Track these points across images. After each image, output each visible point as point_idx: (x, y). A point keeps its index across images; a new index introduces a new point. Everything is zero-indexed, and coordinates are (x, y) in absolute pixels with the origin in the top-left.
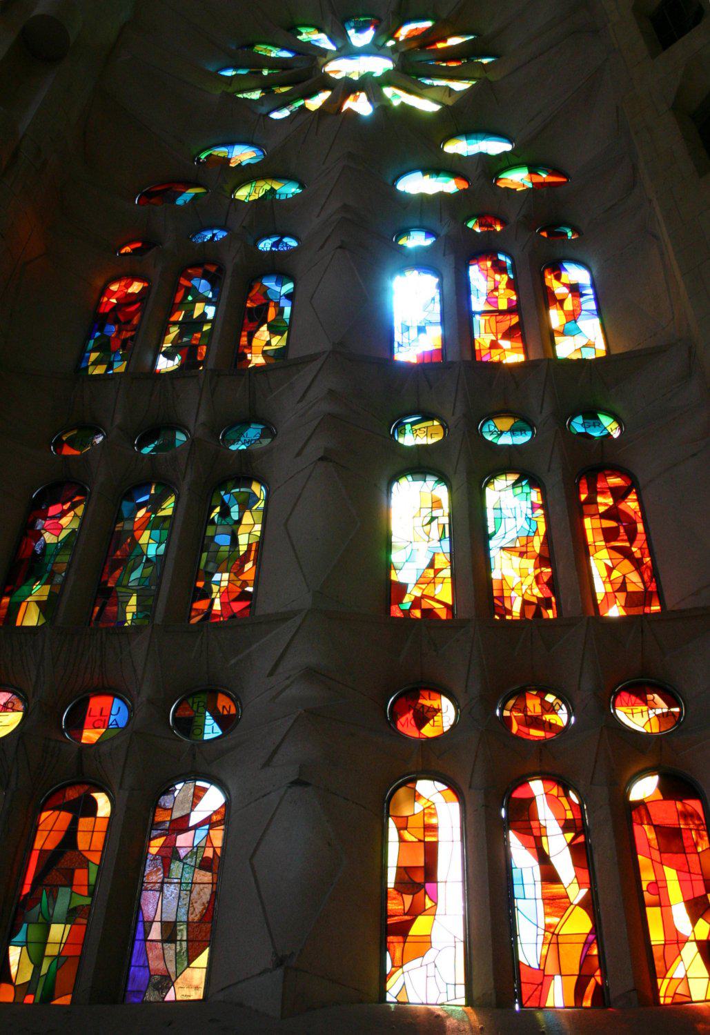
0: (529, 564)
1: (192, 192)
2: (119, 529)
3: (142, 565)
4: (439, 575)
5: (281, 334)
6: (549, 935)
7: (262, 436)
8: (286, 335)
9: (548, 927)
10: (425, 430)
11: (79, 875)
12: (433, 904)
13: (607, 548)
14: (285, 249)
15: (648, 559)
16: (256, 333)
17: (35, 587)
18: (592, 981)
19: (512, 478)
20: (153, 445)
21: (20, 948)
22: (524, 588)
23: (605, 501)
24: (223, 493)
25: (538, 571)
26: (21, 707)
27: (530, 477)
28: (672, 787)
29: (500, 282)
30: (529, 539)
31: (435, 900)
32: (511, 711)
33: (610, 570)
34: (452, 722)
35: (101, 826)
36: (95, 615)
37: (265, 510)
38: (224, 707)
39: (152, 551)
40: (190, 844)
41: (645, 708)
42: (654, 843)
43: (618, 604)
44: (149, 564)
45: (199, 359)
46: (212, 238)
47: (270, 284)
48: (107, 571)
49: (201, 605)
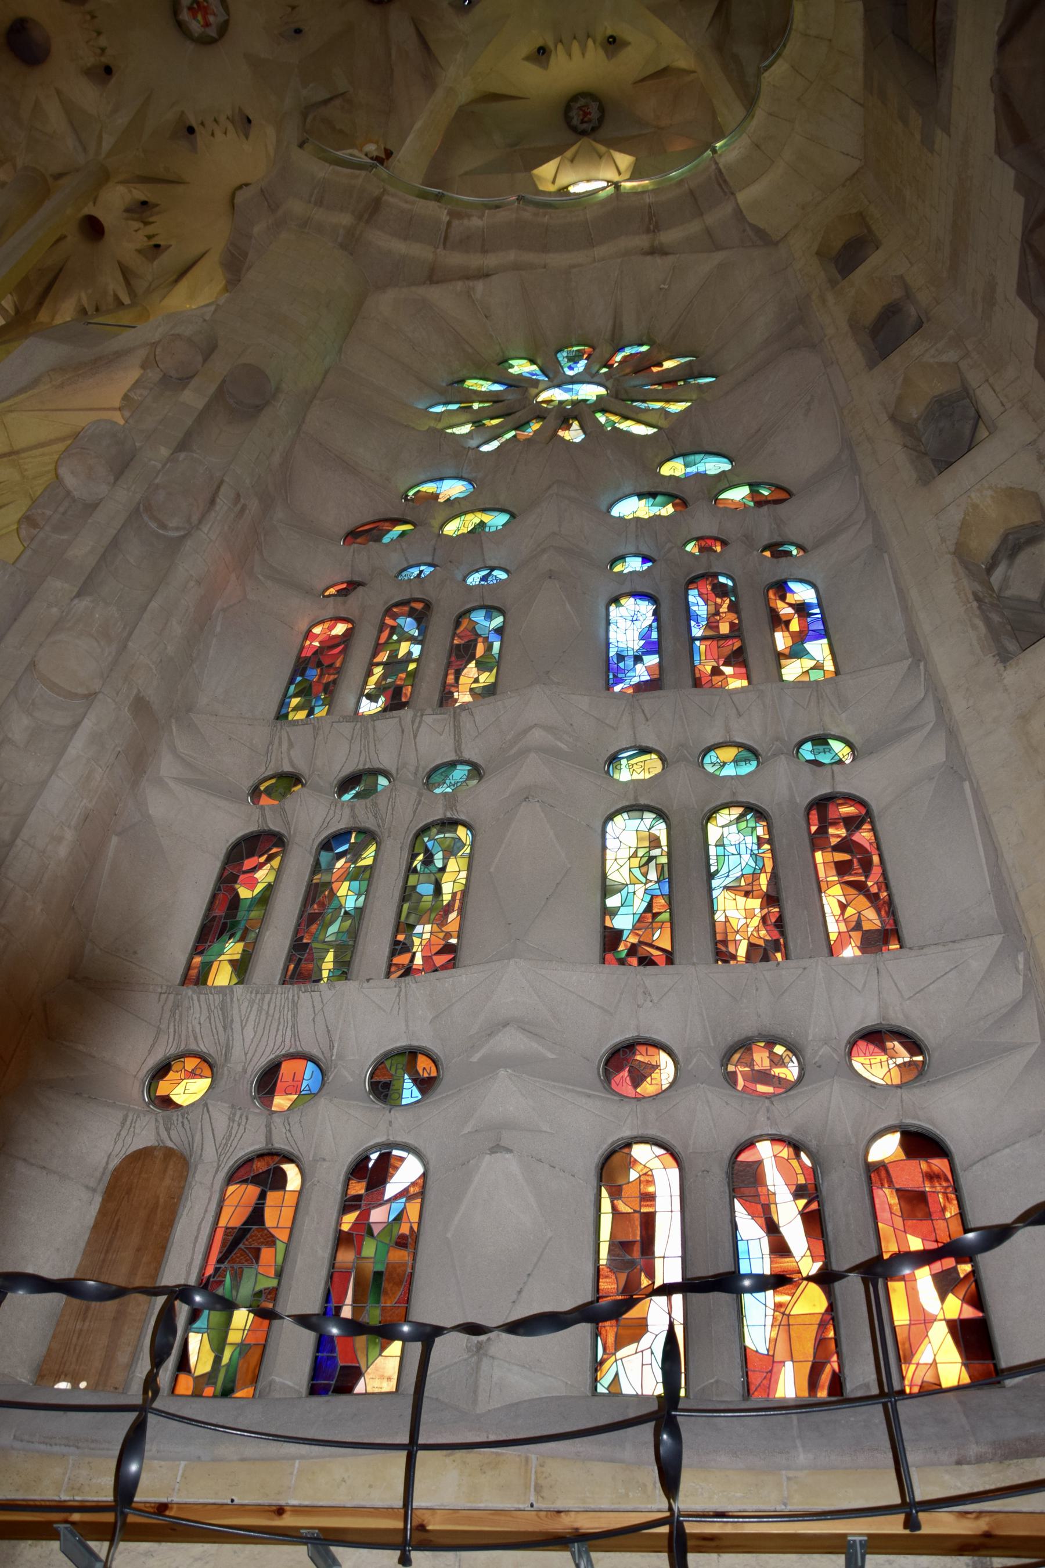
0: (755, 904)
1: (400, 529)
2: (318, 881)
3: (340, 918)
5: (491, 671)
7: (469, 778)
8: (495, 671)
11: (266, 1253)
14: (495, 582)
15: (885, 894)
16: (463, 669)
20: (354, 792)
21: (200, 1335)
22: (750, 930)
23: (836, 833)
24: (426, 839)
25: (765, 911)
29: (721, 606)
30: (755, 876)
32: (736, 1066)
33: (843, 907)
34: (671, 1079)
35: (290, 1200)
36: (289, 973)
37: (471, 857)
38: (424, 1068)
39: (350, 904)
41: (884, 1058)
42: (896, 1209)
43: (853, 944)
45: (403, 700)
46: (419, 575)
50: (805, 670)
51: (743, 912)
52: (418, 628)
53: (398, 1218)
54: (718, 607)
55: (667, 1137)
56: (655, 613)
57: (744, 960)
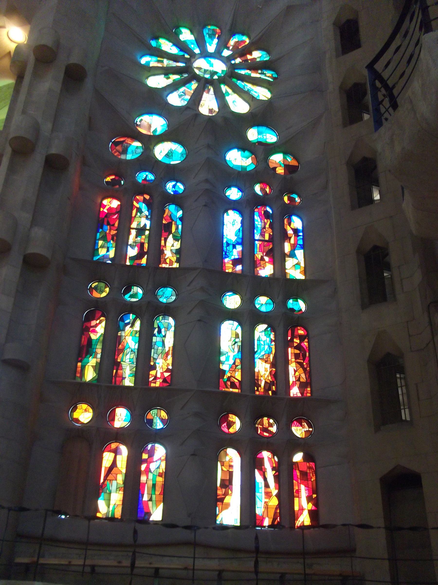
0: (268, 366)
2: (120, 335)
4: (237, 368)
5: (178, 240)
6: (265, 505)
9: (265, 502)
12: (231, 492)
13: (295, 362)
17: (90, 359)
19: (265, 326)
22: (266, 376)
25: (271, 369)
26: (91, 410)
27: (272, 327)
28: (308, 458)
31: (232, 491)
32: (258, 425)
33: (295, 371)
38: (163, 416)
41: (301, 428)
44: (132, 353)
47: (172, 208)
48: (117, 354)
49: (153, 373)
50: (294, 264)
52: (148, 211)
53: (158, 468)
54: (265, 224)
56: (242, 222)
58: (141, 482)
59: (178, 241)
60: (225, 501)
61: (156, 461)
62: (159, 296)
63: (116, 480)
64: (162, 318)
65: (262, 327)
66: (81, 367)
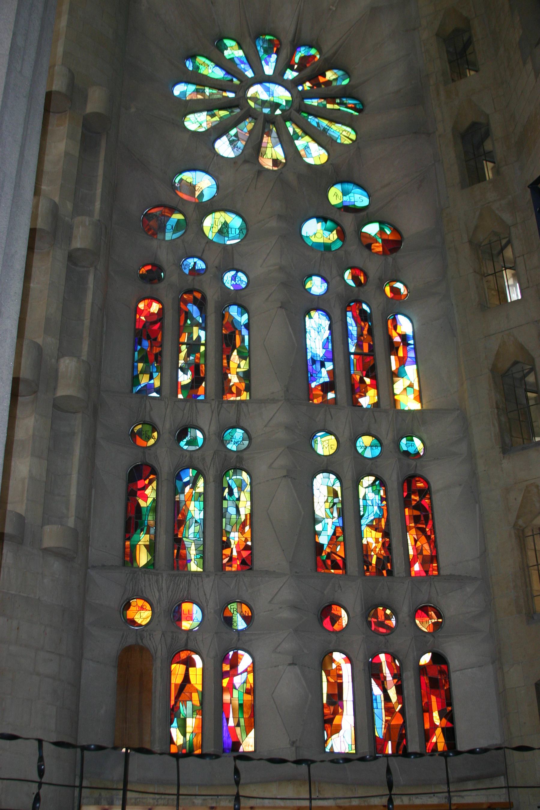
0: (379, 535)
2: (178, 499)
3: (194, 524)
10: (328, 442)
18: (402, 744)
19: (372, 479)
22: (377, 549)
25: (384, 540)
26: (148, 607)
30: (379, 520)
31: (342, 708)
33: (416, 541)
34: (346, 623)
35: (200, 672)
36: (175, 555)
38: (245, 611)
40: (240, 682)
41: (428, 619)
42: (428, 684)
49: (227, 552)
51: (374, 539)
53: (245, 682)
54: (362, 329)
55: (347, 651)
57: (375, 566)
58: (224, 701)
59: (246, 360)
60: (333, 723)
61: (241, 673)
62: (226, 441)
63: (191, 700)
64: (233, 473)
65: (368, 480)
66: (130, 548)
